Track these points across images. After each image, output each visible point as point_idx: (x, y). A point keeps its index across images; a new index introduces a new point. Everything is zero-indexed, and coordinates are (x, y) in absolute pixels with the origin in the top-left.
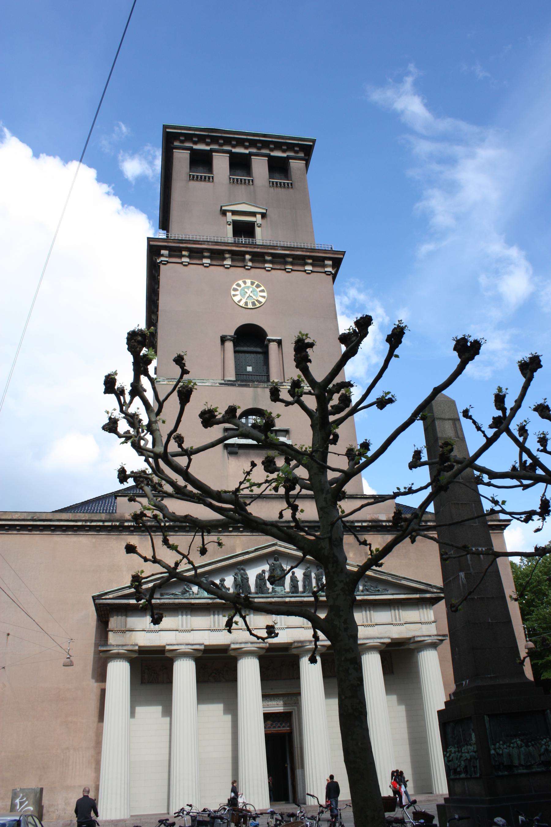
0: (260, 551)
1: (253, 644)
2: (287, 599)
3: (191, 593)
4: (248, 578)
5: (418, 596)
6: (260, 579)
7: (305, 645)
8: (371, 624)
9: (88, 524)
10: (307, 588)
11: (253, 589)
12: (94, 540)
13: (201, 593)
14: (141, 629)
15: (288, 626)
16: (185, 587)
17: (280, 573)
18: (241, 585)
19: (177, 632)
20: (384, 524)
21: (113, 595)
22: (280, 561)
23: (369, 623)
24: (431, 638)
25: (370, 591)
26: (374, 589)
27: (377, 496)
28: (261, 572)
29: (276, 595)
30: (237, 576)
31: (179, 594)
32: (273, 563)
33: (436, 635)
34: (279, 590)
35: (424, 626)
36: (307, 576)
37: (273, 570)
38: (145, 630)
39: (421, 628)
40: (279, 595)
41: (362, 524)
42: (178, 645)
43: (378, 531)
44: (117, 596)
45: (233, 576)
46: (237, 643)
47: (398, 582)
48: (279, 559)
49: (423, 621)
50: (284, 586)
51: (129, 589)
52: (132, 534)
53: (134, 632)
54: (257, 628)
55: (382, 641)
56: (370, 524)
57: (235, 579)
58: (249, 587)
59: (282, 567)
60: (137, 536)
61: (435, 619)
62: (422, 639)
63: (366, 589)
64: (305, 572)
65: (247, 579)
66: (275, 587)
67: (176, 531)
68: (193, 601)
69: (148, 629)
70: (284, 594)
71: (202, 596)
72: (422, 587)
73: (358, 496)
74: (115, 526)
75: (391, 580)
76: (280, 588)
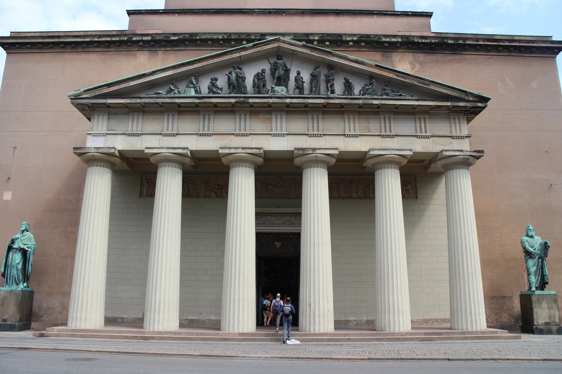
0: (260, 48)
1: (245, 150)
2: (288, 101)
3: (176, 91)
4: (245, 78)
5: (449, 104)
6: (259, 79)
7: (307, 152)
8: (390, 134)
9: (96, 39)
10: (314, 89)
13: (187, 92)
14: (122, 133)
15: (289, 132)
16: (171, 86)
17: (283, 72)
18: (236, 84)
19: (161, 136)
21: (90, 94)
22: (285, 60)
23: (388, 133)
24: (462, 154)
26: (395, 94)
27: (410, 13)
29: (274, 94)
30: (232, 75)
31: (164, 93)
32: (275, 63)
34: (279, 90)
35: (455, 141)
36: (315, 76)
37: (275, 70)
38: (126, 133)
39: (452, 143)
40: (278, 95)
41: (390, 40)
42: (158, 148)
43: (409, 48)
44: (95, 95)
45: (227, 75)
46: (226, 148)
47: (425, 86)
48: (283, 58)
49: (454, 134)
50: (286, 87)
51: (108, 87)
52: (141, 49)
55: (402, 153)
56: (400, 40)
57: (229, 78)
58: (245, 87)
59: (285, 66)
65: (244, 79)
66: (275, 87)
67: (186, 45)
68: (177, 101)
70: (285, 94)
71: (188, 95)
72: (455, 94)
73: (389, 13)
74: (123, 41)
75: (416, 84)
76: (280, 87)
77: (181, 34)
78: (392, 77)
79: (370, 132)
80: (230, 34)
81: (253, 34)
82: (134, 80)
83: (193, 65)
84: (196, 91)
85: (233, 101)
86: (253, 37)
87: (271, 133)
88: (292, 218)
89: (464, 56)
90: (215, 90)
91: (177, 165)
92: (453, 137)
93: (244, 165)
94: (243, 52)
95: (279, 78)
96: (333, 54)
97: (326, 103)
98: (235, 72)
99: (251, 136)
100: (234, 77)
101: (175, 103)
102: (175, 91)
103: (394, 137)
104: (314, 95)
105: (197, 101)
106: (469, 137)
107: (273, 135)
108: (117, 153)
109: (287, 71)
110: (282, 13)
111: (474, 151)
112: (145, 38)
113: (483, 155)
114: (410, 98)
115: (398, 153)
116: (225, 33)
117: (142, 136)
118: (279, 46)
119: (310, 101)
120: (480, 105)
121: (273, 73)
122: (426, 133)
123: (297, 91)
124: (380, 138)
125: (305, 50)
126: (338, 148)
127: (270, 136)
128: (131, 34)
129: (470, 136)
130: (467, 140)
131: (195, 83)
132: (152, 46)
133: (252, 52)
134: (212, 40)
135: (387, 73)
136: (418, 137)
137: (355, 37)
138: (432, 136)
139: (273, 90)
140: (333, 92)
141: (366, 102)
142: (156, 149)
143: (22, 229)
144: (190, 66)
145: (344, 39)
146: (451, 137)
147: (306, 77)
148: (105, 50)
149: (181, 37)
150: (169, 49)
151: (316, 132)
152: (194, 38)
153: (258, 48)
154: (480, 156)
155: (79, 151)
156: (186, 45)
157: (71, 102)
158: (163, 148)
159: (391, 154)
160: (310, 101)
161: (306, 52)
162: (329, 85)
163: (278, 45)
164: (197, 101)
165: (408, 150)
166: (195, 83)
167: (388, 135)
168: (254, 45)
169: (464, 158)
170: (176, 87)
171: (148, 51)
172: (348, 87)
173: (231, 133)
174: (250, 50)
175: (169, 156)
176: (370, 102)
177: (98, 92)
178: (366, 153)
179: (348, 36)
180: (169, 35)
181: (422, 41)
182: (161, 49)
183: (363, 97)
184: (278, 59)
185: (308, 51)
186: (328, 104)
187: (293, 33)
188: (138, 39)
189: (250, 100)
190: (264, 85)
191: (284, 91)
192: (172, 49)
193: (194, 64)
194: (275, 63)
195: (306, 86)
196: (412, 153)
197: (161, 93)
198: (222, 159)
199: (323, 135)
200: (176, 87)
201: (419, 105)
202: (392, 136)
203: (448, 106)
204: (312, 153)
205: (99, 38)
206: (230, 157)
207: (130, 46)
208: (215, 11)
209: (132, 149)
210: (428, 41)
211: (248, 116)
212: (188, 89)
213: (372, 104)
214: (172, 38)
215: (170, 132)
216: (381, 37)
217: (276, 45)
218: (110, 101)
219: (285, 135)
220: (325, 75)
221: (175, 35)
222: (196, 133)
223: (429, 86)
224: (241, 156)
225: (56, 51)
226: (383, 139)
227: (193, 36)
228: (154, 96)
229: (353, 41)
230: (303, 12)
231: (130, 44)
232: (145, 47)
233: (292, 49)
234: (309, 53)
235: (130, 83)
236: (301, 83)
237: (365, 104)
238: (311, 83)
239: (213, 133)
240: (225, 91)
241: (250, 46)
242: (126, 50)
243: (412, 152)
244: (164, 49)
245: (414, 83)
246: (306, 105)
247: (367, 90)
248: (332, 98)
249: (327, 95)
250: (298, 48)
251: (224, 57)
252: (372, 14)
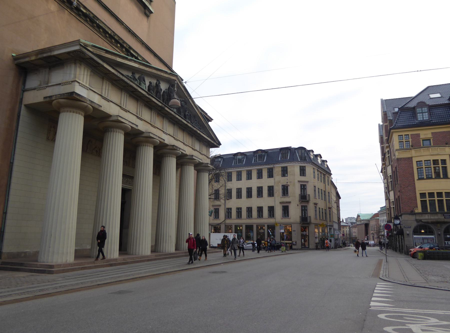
51: (106, 53)
80: (116, 34)
81: (126, 43)
83: (147, 68)
85: (160, 104)
86: (125, 45)
110: (134, 36)
116: (113, 32)
134: (104, 30)
149: (87, 13)
150: (74, 14)
156: (86, 21)
168: (170, 73)
187: (143, 58)
192: (74, 15)
193: (147, 67)
208: (105, 7)
209: (104, 111)
213: (197, 132)
214: (82, 9)
218: (106, 66)
221: (85, 8)
230: (143, 43)
235: (117, 58)
244: (70, 12)
252: (166, 65)
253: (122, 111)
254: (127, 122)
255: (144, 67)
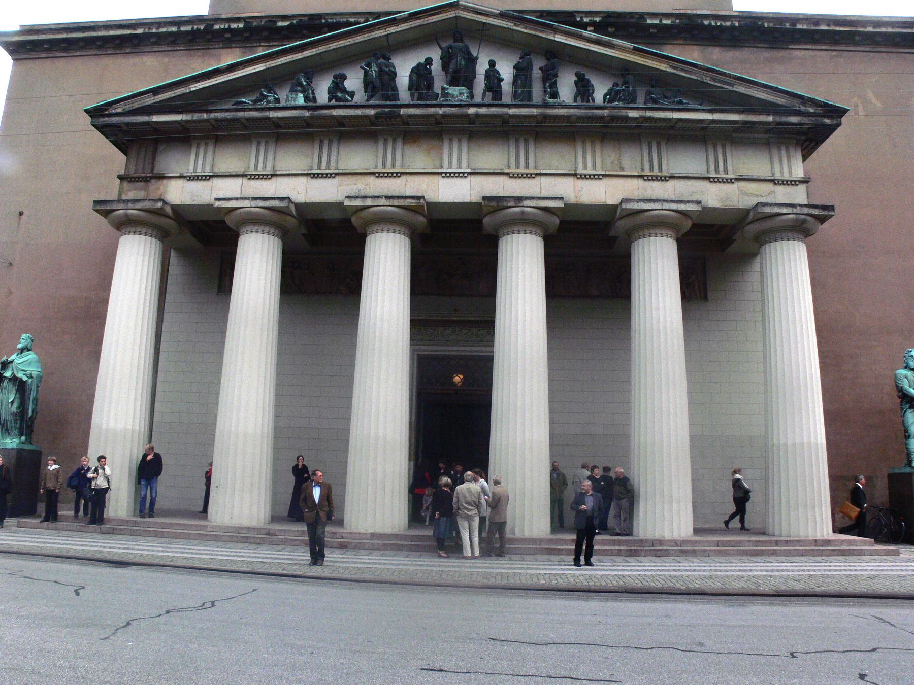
1: (391, 200)
2: (472, 111)
4: (395, 74)
5: (770, 119)
7: (505, 204)
8: (659, 174)
11: (404, 95)
12: (166, 60)
13: (290, 99)
14: (178, 174)
15: (474, 169)
17: (463, 63)
18: (378, 84)
19: (245, 180)
20: (706, 23)
22: (467, 42)
23: (656, 172)
24: (795, 210)
25: (660, 103)
28: (423, 61)
33: (806, 206)
34: (456, 93)
35: (780, 189)
39: (774, 192)
40: (453, 102)
41: (661, 21)
42: (237, 199)
45: (361, 67)
49: (778, 176)
50: (470, 86)
52: (229, 45)
53: (165, 181)
54: (408, 171)
55: (682, 207)
57: (366, 74)
58: (395, 89)
59: (469, 53)
60: (237, 49)
61: (805, 175)
62: (776, 210)
63: (652, 98)
64: (519, 62)
68: (272, 114)
69: (190, 174)
71: (293, 104)
72: (781, 100)
75: (709, 82)
77: (294, 16)
78: (664, 69)
79: (622, 169)
82: (199, 81)
83: (302, 52)
84: (306, 99)
85: (372, 112)
87: (440, 171)
88: (482, 332)
89: (792, 51)
90: (339, 95)
91: (272, 230)
92: (777, 182)
93: (392, 228)
94: (392, 28)
95: (456, 71)
96: (555, 29)
97: (541, 114)
98: (377, 65)
99: (404, 178)
100: (375, 71)
101: (269, 119)
102: (269, 99)
103: (667, 180)
104: (521, 101)
105: (307, 114)
106: (807, 182)
107: (444, 175)
108: (168, 210)
109: (472, 61)
111: (816, 207)
112: (234, 26)
113: (833, 214)
114: (699, 107)
115: (674, 206)
117: (211, 180)
118: (456, 17)
119: (512, 111)
120: (828, 121)
121: (445, 67)
122: (727, 174)
123: (489, 95)
124: (641, 181)
125: (504, 22)
126: (563, 198)
127: (439, 178)
128: (210, 20)
129: (807, 180)
130: (802, 188)
131: (305, 83)
132: (247, 39)
133: (408, 27)
135: (656, 63)
136: (712, 180)
137: (598, 17)
138: (737, 179)
139: (445, 95)
140: (555, 95)
141: (615, 112)
142: (234, 201)
143: (19, 346)
144: (297, 55)
145: (578, 19)
146: (773, 181)
147: (506, 70)
148: (169, 49)
151: (522, 170)
152: (317, 22)
153: (419, 21)
154: (826, 216)
155: (102, 208)
157: (91, 122)
158: (246, 199)
159: (662, 210)
160: (512, 111)
161: (507, 27)
162: (548, 84)
163: (455, 15)
164: (307, 114)
165: (692, 202)
166: (305, 83)
167: (656, 177)
169: (797, 219)
170: (272, 92)
171: (239, 47)
172: (583, 89)
173: (369, 171)
174: (405, 25)
175: (257, 214)
176: (623, 113)
177: (136, 103)
178: (614, 208)
179: (584, 15)
180: (274, 19)
181: (716, 23)
182: (263, 44)
183: (609, 104)
184: (455, 41)
185: (510, 24)
186: (546, 117)
188: (222, 27)
189: (403, 111)
190: (430, 86)
191: (465, 95)
194: (450, 47)
195: (506, 86)
196: (700, 209)
197: (245, 102)
198: (352, 219)
199: (537, 174)
200: (272, 92)
201: (713, 121)
202: (663, 178)
203: (768, 123)
204: (514, 205)
205: (158, 28)
206: (364, 214)
207: (209, 40)
209: (193, 203)
210: (728, 24)
211: (399, 144)
212: (292, 94)
213: (627, 118)
214: (280, 24)
215: (260, 171)
216: (646, 16)
217: (451, 14)
218: (156, 118)
219: (466, 175)
220: (541, 69)
221: (284, 18)
222: (305, 172)
223: (733, 87)
224: (384, 212)
225: (90, 53)
226: (647, 184)
227: (316, 20)
228: (234, 107)
229: (593, 24)
231: (209, 36)
232: (235, 42)
233: (481, 20)
234: (512, 28)
235: (191, 86)
236: (496, 81)
237: (613, 118)
238: (515, 82)
239: (337, 171)
240: (360, 97)
241: (403, 16)
242: (203, 47)
243: (700, 205)
245: (705, 81)
246: (505, 120)
247: (618, 92)
248: (553, 106)
249: (544, 100)
250: (492, 20)
251: (358, 38)
253: (253, 182)
254: (246, 203)
255: (291, 57)
